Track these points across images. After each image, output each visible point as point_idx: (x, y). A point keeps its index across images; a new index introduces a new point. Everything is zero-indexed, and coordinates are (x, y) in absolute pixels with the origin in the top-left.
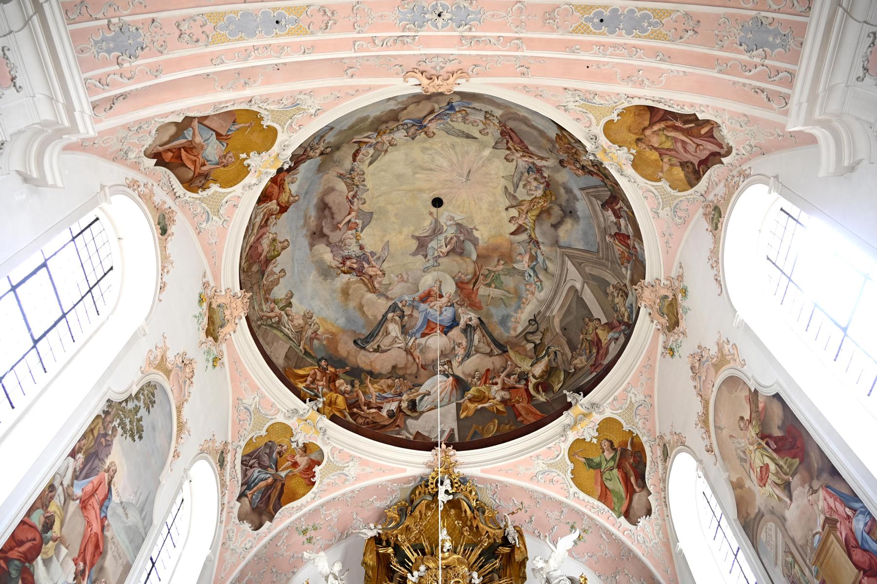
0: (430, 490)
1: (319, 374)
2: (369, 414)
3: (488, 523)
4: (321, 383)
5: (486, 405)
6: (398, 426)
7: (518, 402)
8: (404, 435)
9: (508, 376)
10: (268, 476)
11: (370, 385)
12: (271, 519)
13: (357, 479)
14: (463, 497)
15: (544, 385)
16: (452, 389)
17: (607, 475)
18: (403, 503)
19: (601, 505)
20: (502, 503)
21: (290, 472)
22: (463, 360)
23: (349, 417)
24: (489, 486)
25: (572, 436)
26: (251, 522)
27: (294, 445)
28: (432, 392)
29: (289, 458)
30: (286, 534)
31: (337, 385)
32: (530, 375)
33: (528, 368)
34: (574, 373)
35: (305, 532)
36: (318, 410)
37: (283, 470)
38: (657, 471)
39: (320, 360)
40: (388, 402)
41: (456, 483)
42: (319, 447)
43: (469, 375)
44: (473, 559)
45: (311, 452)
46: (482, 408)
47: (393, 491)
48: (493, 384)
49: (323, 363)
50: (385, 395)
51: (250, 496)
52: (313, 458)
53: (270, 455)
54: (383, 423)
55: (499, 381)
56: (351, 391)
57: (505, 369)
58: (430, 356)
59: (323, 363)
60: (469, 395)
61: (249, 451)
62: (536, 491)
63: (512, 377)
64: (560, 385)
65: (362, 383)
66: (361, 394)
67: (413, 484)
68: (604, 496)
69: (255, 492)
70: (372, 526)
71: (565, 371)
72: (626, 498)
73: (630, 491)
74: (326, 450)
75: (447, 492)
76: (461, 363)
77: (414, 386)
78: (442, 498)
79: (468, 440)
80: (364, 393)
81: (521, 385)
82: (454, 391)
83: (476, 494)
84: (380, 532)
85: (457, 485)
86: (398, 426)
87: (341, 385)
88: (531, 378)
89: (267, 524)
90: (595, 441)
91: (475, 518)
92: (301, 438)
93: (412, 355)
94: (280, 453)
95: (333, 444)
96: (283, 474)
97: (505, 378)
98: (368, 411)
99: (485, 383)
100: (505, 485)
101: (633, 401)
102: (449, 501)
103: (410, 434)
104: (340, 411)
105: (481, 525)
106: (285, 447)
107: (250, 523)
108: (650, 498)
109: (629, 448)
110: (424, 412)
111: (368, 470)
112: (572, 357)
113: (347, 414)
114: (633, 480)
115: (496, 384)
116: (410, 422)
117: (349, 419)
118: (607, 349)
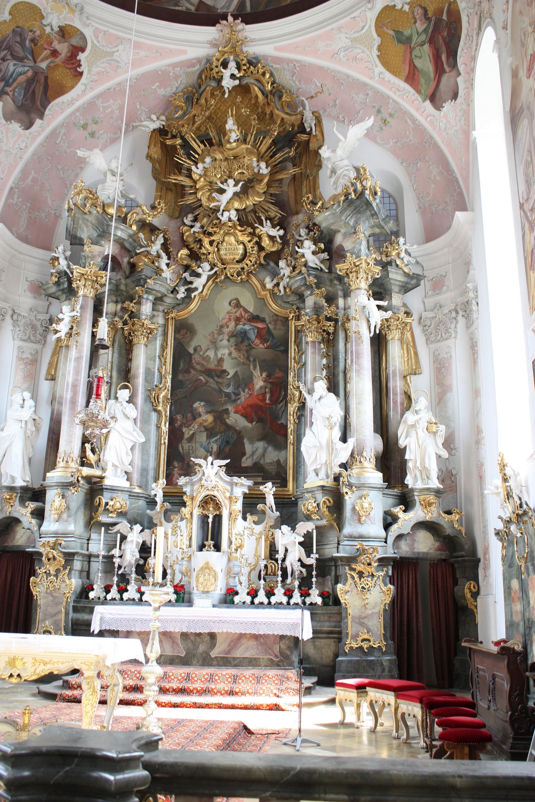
0: (215, 75)
3: (285, 108)
10: (26, 69)
12: (41, 116)
14: (253, 81)
18: (190, 89)
20: (303, 86)
21: (51, 62)
24: (285, 66)
26: (20, 121)
29: (46, 46)
30: (63, 131)
35: (84, 127)
37: (42, 60)
41: (245, 65)
42: (78, 30)
44: (263, 148)
45: (70, 37)
47: (176, 77)
51: (11, 93)
52: (72, 44)
62: (338, 72)
67: (198, 66)
69: (15, 88)
70: (154, 117)
72: (435, 79)
73: (439, 71)
74: (88, 33)
75: (233, 76)
79: (261, 9)
83: (272, 75)
84: (164, 123)
85: (245, 68)
89: (38, 122)
91: (268, 104)
95: (94, 24)
96: (44, 65)
100: (304, 66)
102: (234, 88)
103: (192, 4)
105: (277, 112)
106: (38, 33)
107: (18, 122)
111: (143, 53)
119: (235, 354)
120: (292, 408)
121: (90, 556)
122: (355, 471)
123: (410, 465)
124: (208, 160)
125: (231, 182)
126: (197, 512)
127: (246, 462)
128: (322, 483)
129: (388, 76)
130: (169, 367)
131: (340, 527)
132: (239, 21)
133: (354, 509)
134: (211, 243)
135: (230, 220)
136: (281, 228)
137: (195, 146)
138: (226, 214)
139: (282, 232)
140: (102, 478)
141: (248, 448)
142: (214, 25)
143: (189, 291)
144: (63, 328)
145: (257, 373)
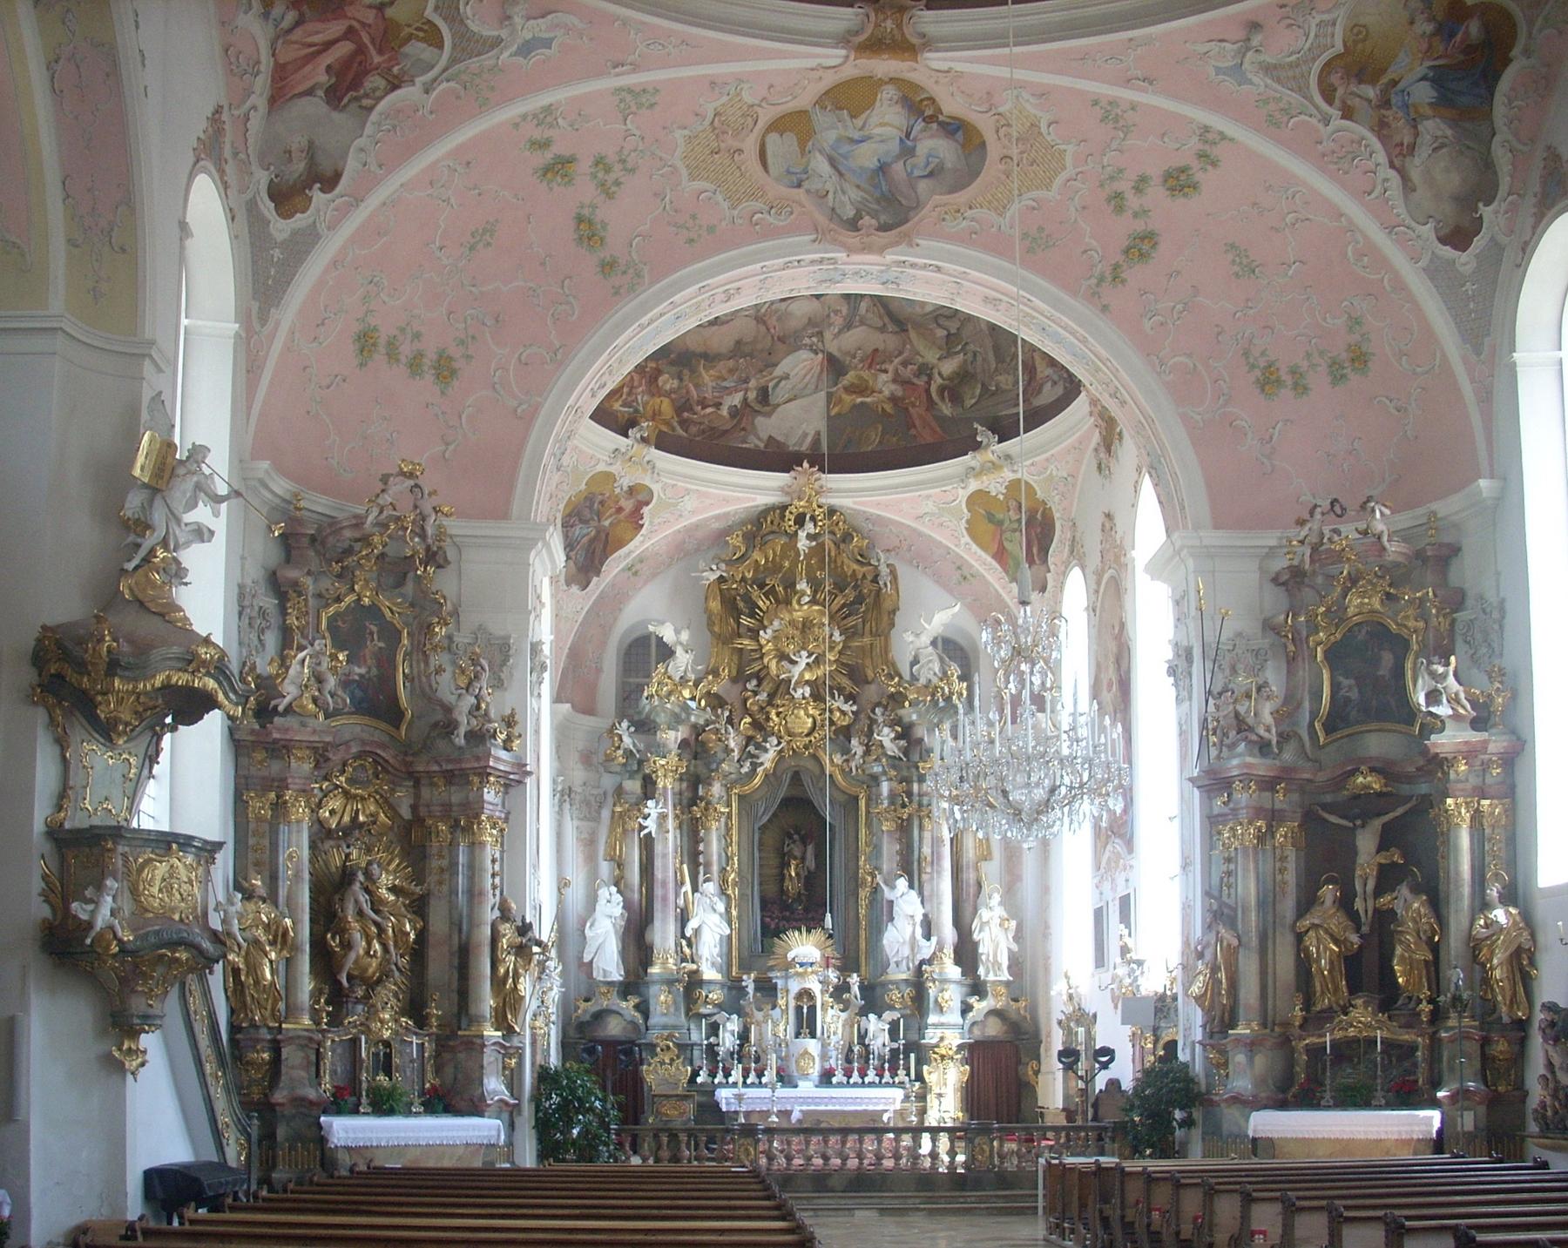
2: (704, 416)
5: (868, 400)
6: (744, 429)
7: (914, 406)
8: (753, 443)
9: (905, 364)
11: (703, 372)
12: (598, 573)
15: (953, 391)
16: (822, 370)
17: (1008, 535)
19: (994, 563)
20: (876, 529)
23: (678, 428)
25: (974, 485)
27: (617, 491)
28: (792, 374)
32: (935, 371)
33: (935, 361)
34: (994, 394)
35: (629, 569)
36: (644, 440)
38: (1061, 552)
40: (730, 394)
43: (848, 353)
46: (862, 403)
50: (725, 384)
53: (591, 508)
54: (725, 428)
55: (891, 368)
56: (679, 388)
57: (900, 353)
58: (794, 324)
61: (567, 512)
63: (910, 367)
64: (973, 401)
65: (693, 371)
66: (692, 388)
68: (1000, 555)
71: (983, 385)
74: (656, 488)
75: (810, 537)
76: (836, 336)
77: (767, 366)
78: (803, 544)
79: (837, 452)
80: (697, 386)
81: (921, 382)
86: (744, 429)
88: (937, 376)
89: (595, 579)
90: (1001, 497)
92: (626, 482)
93: (764, 323)
96: (607, 523)
101: (1054, 473)
103: (759, 439)
104: (667, 423)
105: (846, 561)
108: (1048, 575)
109: (1039, 516)
110: (778, 405)
112: (996, 368)
113: (675, 424)
114: (1035, 550)
115: (886, 371)
116: (760, 420)
117: (680, 431)
118: (1041, 386)
124: (776, 623)
125: (804, 654)
134: (778, 714)
135: (804, 698)
136: (854, 703)
137: (761, 603)
138: (800, 691)
139: (855, 708)
143: (754, 766)
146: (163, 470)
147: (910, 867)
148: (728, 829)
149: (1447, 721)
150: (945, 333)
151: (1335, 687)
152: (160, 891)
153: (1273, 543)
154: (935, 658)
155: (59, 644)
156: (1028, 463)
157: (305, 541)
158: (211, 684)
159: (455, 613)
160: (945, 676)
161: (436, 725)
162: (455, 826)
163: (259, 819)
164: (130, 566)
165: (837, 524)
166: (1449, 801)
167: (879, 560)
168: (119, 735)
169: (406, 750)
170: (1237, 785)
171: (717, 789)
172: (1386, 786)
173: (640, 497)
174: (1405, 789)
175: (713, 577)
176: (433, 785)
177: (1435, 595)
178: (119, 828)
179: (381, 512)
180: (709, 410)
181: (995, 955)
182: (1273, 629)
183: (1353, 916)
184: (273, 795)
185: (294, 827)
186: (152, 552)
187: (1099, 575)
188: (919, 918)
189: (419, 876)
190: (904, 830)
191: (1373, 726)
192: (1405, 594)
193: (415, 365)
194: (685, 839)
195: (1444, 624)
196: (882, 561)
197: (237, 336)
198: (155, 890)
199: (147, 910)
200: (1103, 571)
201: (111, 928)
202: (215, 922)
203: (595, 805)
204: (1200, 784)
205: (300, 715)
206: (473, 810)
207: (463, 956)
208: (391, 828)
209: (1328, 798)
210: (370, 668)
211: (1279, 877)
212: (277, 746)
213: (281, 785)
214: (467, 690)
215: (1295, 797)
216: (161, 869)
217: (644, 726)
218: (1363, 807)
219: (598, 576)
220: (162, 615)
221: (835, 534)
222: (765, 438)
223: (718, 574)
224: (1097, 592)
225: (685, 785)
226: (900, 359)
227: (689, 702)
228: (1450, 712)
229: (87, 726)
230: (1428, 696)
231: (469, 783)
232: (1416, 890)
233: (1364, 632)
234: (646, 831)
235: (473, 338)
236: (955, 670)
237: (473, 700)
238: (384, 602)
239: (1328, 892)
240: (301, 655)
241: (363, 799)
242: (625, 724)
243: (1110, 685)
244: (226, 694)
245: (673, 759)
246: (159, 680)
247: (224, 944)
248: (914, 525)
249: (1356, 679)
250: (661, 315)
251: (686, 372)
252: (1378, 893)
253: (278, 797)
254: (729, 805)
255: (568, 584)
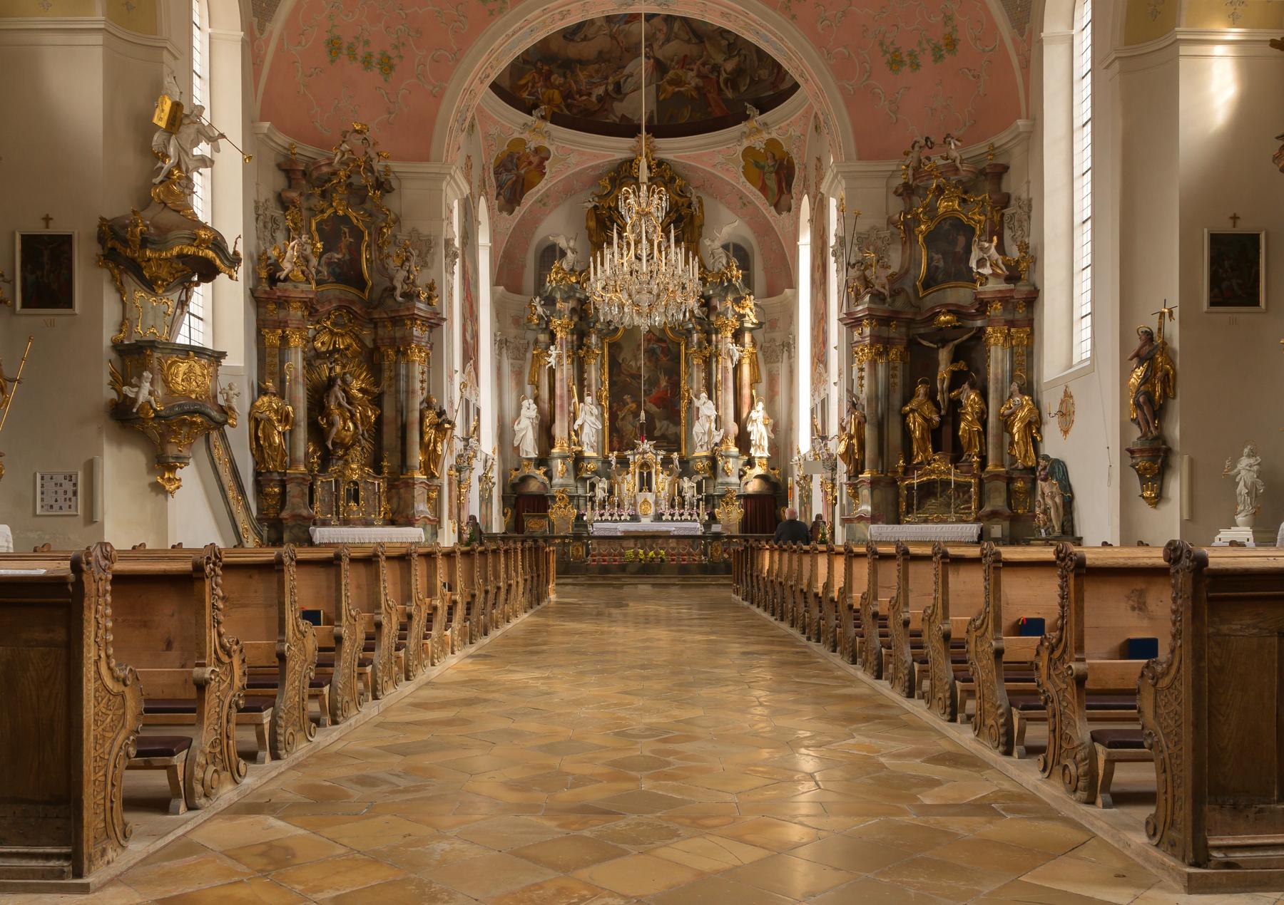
1: (537, 76)
4: (539, 85)
5: (682, 89)
6: (606, 110)
8: (613, 119)
9: (704, 64)
11: (580, 74)
13: (577, 164)
22: (663, 44)
27: (528, 150)
28: (635, 73)
31: (552, 80)
35: (540, 201)
36: (543, 118)
39: (536, 63)
40: (596, 87)
48: (689, 69)
49: (539, 64)
50: (594, 80)
53: (512, 161)
55: (695, 67)
56: (565, 83)
57: (701, 57)
59: (539, 64)
60: (668, 78)
74: (552, 149)
76: (661, 47)
77: (619, 68)
80: (576, 82)
82: (655, 74)
86: (606, 110)
87: (556, 79)
92: (533, 145)
93: (616, 39)
94: (519, 158)
96: (523, 172)
97: (702, 68)
98: (580, 99)
99: (682, 68)
103: (617, 117)
104: (558, 106)
113: (563, 107)
115: (692, 70)
116: (616, 105)
119: (648, 364)
120: (684, 403)
121: (579, 496)
122: (723, 447)
123: (753, 442)
126: (637, 471)
127: (657, 433)
128: (705, 454)
129: (748, 184)
130: (607, 375)
131: (715, 478)
132: (650, 135)
133: (723, 469)
140: (581, 452)
141: (658, 424)
142: (633, 137)
144: (552, 360)
145: (662, 377)
146: (175, 121)
147: (711, 389)
148: (602, 365)
149: (989, 277)
150: (727, 42)
151: (930, 260)
152: (183, 380)
153: (894, 168)
154: (723, 255)
155: (111, 228)
156: (777, 127)
157: (299, 175)
158: (211, 254)
159: (397, 220)
160: (728, 266)
161: (385, 289)
162: (398, 352)
163: (272, 346)
164: (157, 180)
165: (665, 171)
166: (989, 330)
167: (692, 194)
168: (159, 287)
169: (370, 305)
170: (865, 322)
171: (594, 339)
172: (958, 321)
173: (542, 155)
174: (970, 324)
175: (590, 206)
176: (385, 326)
177: (990, 197)
178: (153, 342)
179: (343, 155)
180: (584, 98)
181: (760, 440)
182: (893, 224)
183: (936, 404)
184: (280, 331)
185: (293, 350)
186: (170, 173)
187: (815, 197)
188: (713, 418)
189: (377, 383)
190: (707, 362)
191: (952, 284)
192: (971, 198)
193: (367, 62)
194: (575, 370)
195: (997, 218)
196: (694, 195)
197: (243, 40)
198: (179, 380)
199: (174, 392)
200: (817, 195)
201: (149, 402)
202: (221, 401)
203: (522, 350)
204: (845, 322)
205: (294, 281)
206: (407, 340)
207: (404, 430)
208: (361, 353)
209: (922, 331)
210: (344, 255)
211: (892, 380)
212: (281, 301)
213: (283, 324)
214: (402, 267)
215: (903, 330)
216: (183, 367)
217: (549, 301)
218: (942, 337)
219: (519, 205)
220: (178, 212)
221: (664, 177)
222: (620, 116)
223: (594, 203)
224: (814, 209)
225: (575, 337)
226: (701, 61)
227: (575, 285)
228: (991, 272)
229: (139, 283)
230: (978, 262)
231: (405, 325)
232: (972, 387)
233: (948, 223)
234: (550, 365)
235: (403, 44)
236: (734, 263)
237: (405, 273)
238: (351, 213)
239: (921, 390)
240: (292, 244)
241: (342, 335)
242: (538, 299)
243: (818, 268)
244: (221, 260)
245: (565, 320)
246: (175, 251)
247: (226, 413)
248: (713, 171)
249: (942, 254)
250: (521, 29)
251: (568, 72)
252: (951, 389)
253: (284, 332)
254: (602, 349)
255: (500, 211)
